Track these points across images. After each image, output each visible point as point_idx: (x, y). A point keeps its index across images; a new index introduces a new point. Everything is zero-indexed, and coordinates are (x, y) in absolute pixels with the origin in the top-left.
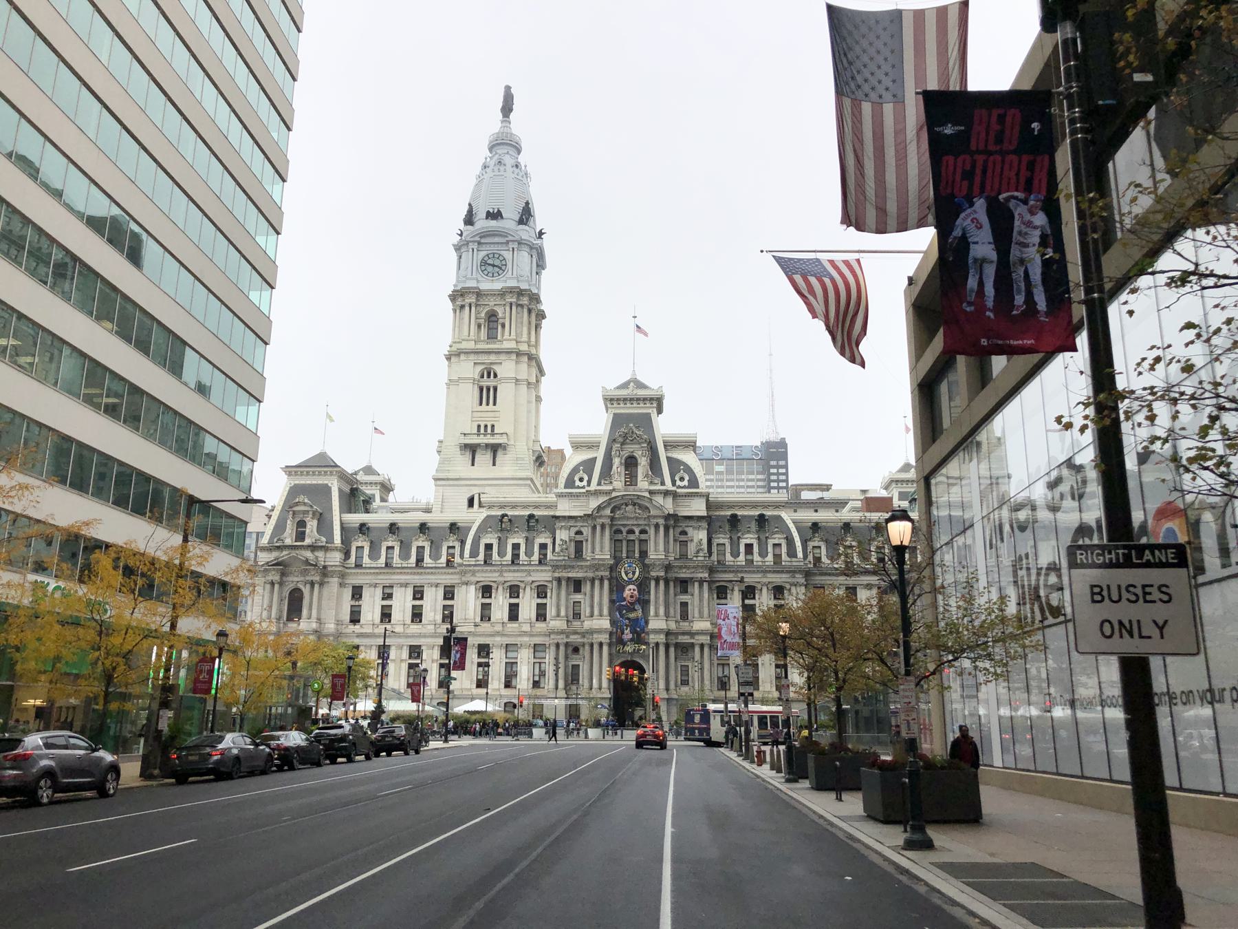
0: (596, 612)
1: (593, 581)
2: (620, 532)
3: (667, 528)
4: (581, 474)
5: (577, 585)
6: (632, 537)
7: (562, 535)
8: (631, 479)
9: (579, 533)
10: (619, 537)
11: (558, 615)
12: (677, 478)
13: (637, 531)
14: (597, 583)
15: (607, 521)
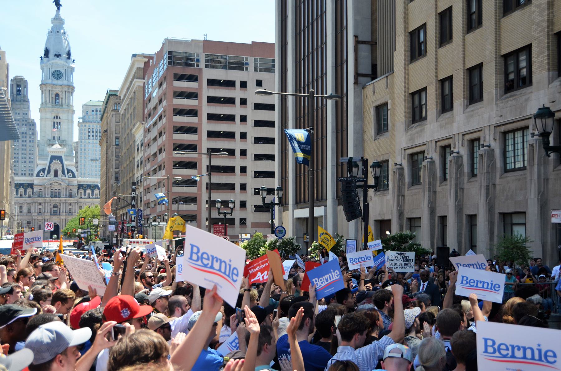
0: (46, 211)
1: (45, 202)
2: (52, 189)
3: (66, 189)
4: (42, 173)
5: (40, 204)
6: (56, 191)
7: (36, 189)
8: (56, 175)
9: (41, 189)
10: (52, 191)
11: (35, 212)
12: (69, 174)
13: (58, 189)
14: (46, 204)
15: (49, 186)
